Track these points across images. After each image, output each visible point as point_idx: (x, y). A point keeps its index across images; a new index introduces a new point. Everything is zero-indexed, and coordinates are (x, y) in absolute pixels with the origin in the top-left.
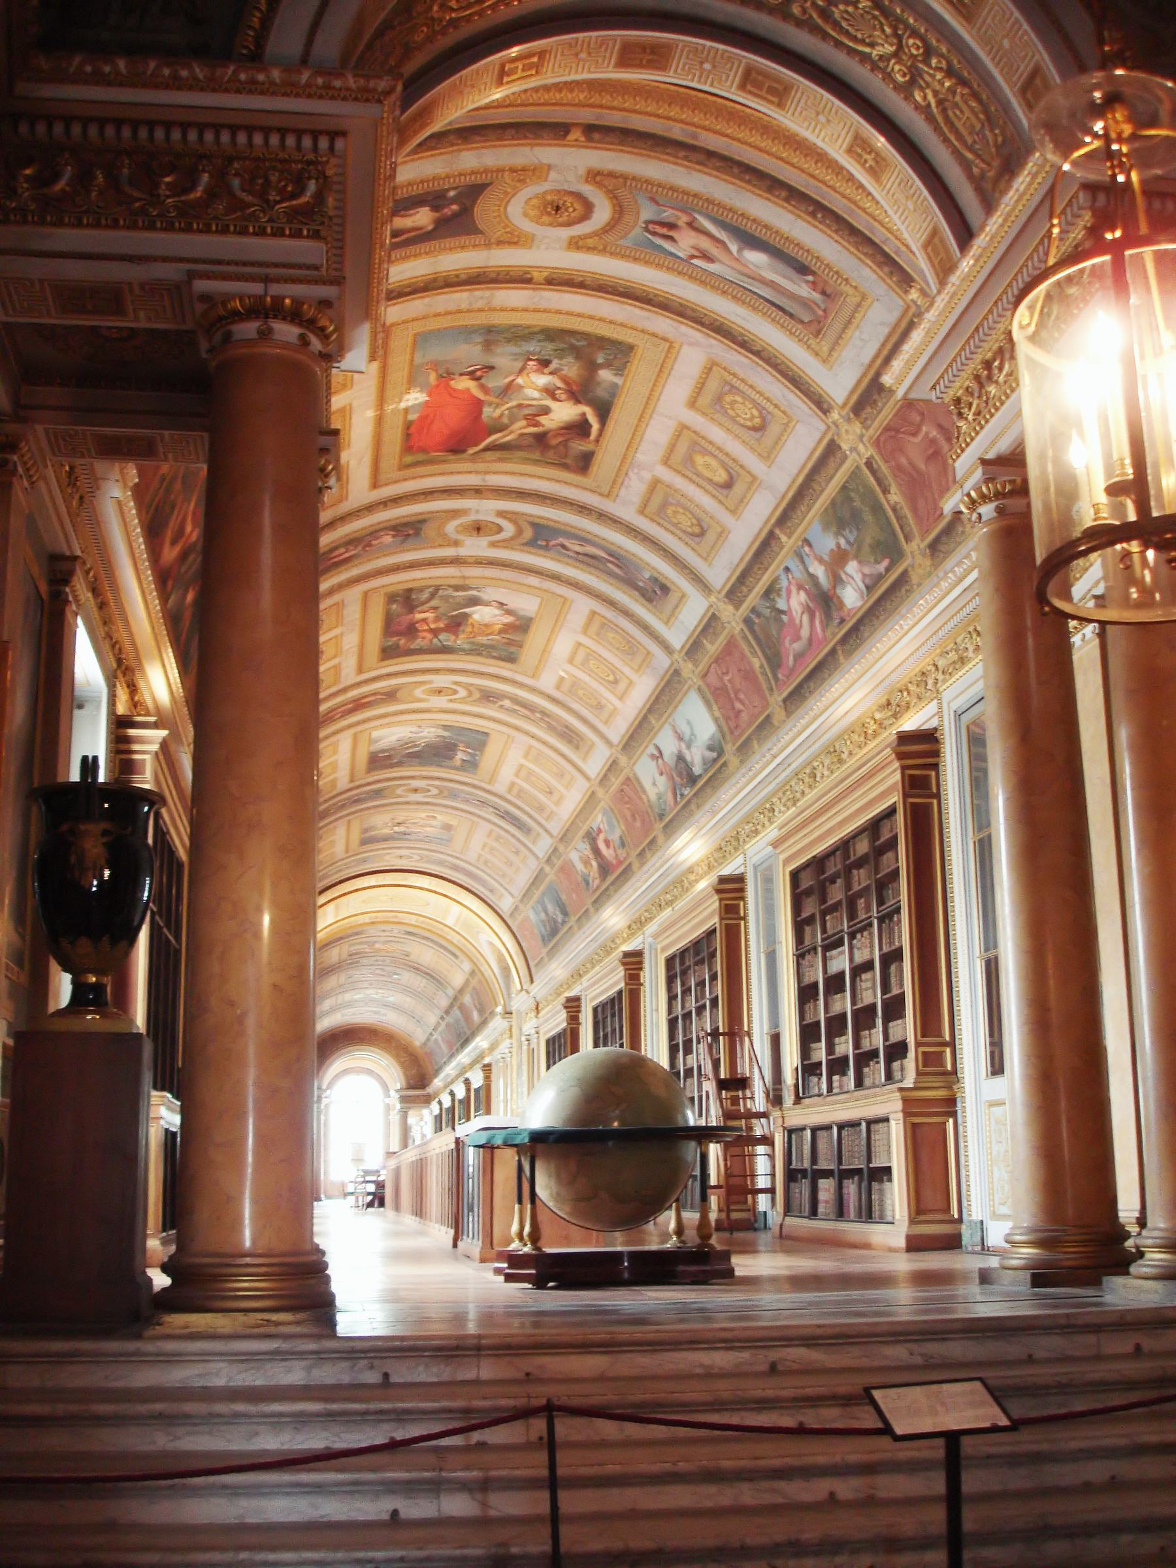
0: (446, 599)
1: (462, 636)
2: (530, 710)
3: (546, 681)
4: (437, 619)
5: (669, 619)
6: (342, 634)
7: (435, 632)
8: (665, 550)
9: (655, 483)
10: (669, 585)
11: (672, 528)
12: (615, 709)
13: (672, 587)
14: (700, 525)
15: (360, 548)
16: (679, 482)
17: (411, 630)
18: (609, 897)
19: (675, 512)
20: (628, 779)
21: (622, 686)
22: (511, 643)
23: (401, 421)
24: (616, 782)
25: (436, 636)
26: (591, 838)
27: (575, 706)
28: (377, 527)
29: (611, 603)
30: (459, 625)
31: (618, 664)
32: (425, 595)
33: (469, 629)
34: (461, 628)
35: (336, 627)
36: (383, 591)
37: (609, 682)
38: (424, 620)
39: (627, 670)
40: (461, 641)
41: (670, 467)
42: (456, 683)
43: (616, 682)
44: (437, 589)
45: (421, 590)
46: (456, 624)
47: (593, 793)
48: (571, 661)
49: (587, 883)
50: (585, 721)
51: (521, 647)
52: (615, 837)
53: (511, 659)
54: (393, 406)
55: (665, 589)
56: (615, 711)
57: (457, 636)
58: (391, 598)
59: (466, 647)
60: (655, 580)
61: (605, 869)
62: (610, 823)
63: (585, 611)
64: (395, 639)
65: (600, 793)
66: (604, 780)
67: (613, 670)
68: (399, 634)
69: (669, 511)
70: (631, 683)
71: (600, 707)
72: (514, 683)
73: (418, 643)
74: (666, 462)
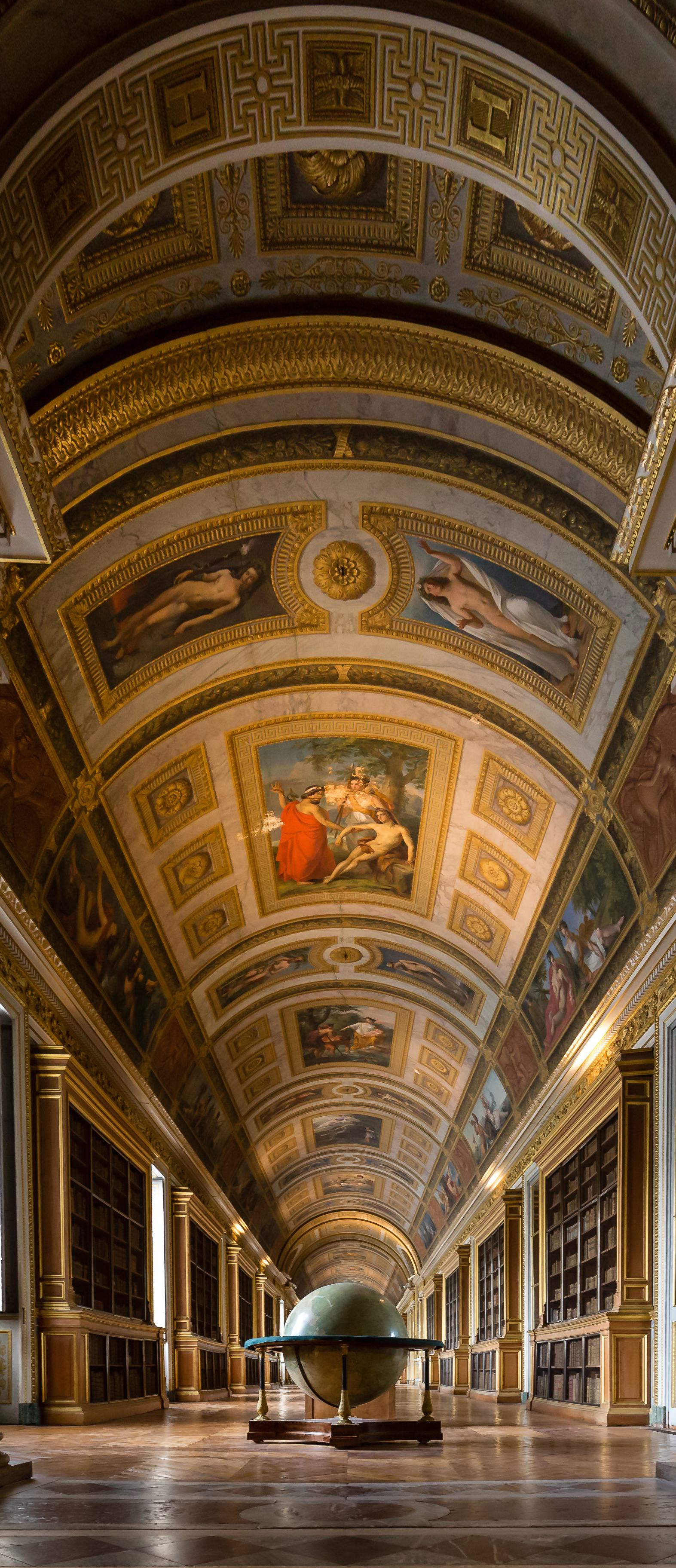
0: (337, 1016)
1: (352, 1047)
2: (402, 1101)
3: (408, 1079)
4: (334, 1034)
5: (475, 1017)
6: (273, 1043)
7: (335, 1044)
8: (468, 959)
9: (458, 896)
10: (473, 989)
11: (471, 938)
12: (449, 1092)
13: (475, 990)
14: (490, 931)
15: (267, 971)
16: (473, 893)
17: (319, 1043)
18: (455, 1216)
19: (472, 923)
20: (460, 1140)
21: (452, 1075)
22: (383, 1051)
23: (268, 847)
24: (454, 1144)
25: (336, 1048)
26: (444, 1182)
27: (427, 1094)
28: (275, 953)
29: (439, 1011)
30: (349, 1039)
31: (448, 1059)
32: (322, 1015)
33: (356, 1042)
34: (351, 1041)
35: (267, 1037)
36: (293, 1010)
37: (445, 1074)
38: (326, 1035)
39: (453, 1063)
40: (352, 1051)
41: (466, 879)
42: (356, 1084)
43: (448, 1073)
44: (329, 1009)
45: (319, 1009)
46: (348, 1037)
47: (442, 1153)
48: (420, 1062)
49: (444, 1209)
50: (433, 1105)
51: (388, 1052)
52: (456, 1180)
53: (385, 1063)
54: (256, 832)
55: (471, 992)
56: (449, 1094)
57: (349, 1047)
58: (300, 1016)
59: (357, 1055)
60: (464, 986)
61: (452, 1201)
62: (453, 1173)
63: (424, 1020)
64: (310, 1050)
65: (446, 1153)
66: (447, 1144)
67: (446, 1064)
68: (312, 1046)
69: (469, 922)
70: (456, 1072)
71: (440, 1093)
72: (389, 1081)
73: (326, 1053)
74: (462, 876)
